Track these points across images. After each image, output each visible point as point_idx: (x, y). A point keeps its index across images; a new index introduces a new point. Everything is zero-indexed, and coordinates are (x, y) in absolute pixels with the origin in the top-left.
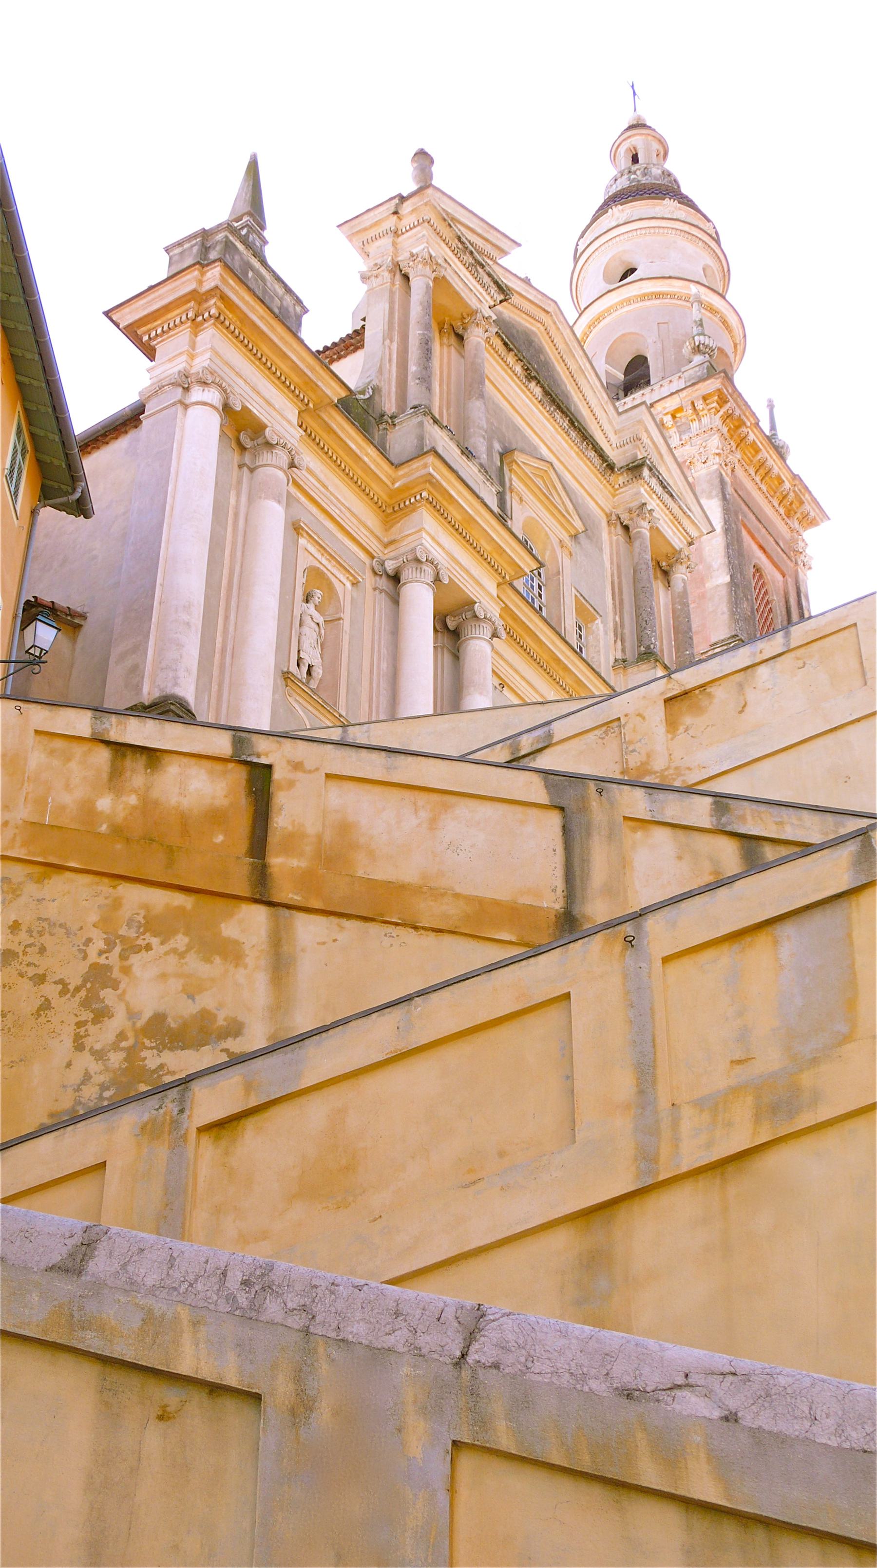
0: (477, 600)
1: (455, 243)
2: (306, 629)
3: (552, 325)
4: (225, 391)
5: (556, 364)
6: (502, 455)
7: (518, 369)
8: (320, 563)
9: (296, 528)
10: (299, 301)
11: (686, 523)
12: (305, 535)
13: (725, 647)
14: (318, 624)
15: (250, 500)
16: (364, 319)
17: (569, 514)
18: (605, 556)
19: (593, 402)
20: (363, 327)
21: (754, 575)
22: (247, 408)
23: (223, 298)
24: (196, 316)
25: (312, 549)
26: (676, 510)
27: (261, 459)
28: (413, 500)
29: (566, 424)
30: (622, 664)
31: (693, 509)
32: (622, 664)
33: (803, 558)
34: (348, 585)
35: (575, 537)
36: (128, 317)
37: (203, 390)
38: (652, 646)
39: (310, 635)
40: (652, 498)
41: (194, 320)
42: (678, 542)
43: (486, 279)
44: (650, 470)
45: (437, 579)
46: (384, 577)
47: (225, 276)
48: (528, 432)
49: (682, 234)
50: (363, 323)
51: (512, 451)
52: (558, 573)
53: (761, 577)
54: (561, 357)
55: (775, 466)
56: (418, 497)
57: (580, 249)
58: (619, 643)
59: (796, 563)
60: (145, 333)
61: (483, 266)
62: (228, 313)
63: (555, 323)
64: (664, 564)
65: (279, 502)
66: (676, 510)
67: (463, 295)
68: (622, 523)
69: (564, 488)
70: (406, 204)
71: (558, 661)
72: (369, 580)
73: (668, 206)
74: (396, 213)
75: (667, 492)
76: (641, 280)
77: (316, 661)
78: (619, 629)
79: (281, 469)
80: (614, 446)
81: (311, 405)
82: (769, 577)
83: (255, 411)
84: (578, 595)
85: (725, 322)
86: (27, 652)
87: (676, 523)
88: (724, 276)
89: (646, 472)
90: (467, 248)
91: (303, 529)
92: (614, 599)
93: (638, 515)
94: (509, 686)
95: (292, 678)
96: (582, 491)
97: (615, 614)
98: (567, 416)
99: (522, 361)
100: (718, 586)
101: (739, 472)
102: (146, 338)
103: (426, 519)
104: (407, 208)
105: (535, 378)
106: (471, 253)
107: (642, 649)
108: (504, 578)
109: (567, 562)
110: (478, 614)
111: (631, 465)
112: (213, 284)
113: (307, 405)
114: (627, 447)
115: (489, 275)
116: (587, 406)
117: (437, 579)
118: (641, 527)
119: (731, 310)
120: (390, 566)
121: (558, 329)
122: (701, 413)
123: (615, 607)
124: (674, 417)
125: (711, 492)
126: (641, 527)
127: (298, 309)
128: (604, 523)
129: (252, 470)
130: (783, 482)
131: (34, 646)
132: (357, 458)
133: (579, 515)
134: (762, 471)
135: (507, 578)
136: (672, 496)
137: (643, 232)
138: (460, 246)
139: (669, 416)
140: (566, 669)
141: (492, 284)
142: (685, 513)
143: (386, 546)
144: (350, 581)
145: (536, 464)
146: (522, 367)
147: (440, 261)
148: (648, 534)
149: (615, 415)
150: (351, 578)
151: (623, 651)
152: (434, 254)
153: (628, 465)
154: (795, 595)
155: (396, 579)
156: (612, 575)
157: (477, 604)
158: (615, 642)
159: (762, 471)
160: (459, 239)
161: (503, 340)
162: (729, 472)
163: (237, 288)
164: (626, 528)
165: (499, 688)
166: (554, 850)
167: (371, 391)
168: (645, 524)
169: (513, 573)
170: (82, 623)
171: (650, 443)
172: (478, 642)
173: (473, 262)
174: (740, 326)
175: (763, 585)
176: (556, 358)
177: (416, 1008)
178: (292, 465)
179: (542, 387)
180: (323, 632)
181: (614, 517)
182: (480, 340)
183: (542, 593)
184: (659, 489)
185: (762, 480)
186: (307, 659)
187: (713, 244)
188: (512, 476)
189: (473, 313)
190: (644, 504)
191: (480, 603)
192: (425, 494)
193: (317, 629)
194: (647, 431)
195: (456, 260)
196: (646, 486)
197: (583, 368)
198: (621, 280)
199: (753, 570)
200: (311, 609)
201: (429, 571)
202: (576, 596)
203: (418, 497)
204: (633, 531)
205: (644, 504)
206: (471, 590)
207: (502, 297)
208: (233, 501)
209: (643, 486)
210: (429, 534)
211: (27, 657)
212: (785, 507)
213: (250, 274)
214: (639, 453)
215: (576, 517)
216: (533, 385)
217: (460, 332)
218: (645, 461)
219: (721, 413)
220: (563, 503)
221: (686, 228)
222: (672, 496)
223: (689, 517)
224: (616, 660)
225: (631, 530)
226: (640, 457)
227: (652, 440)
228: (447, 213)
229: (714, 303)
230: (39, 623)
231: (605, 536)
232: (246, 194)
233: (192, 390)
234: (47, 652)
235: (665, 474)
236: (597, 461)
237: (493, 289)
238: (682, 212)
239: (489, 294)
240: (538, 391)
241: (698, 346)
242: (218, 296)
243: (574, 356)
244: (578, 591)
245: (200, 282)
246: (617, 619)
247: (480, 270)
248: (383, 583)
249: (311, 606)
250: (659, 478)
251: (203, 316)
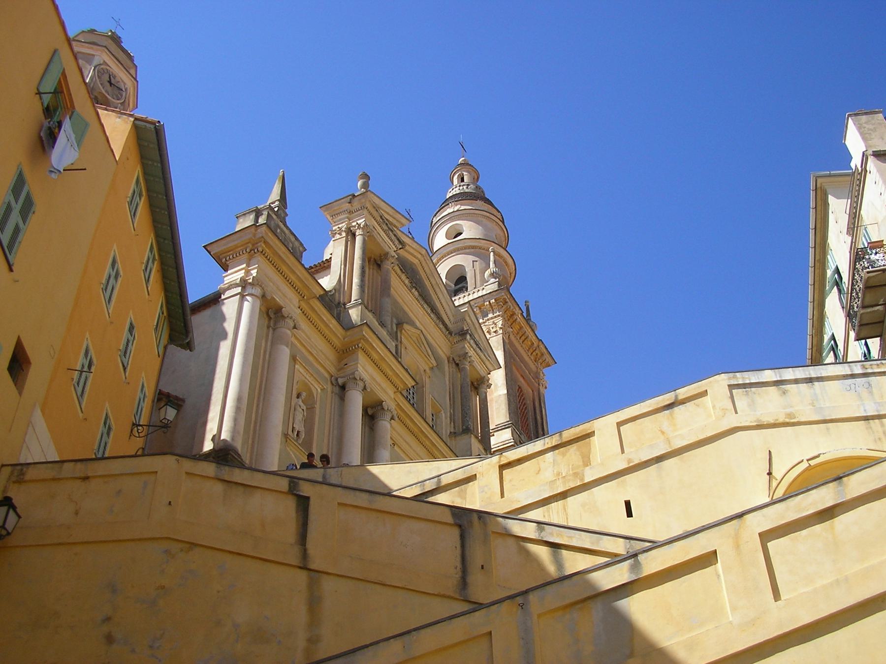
0: (384, 400)
1: (379, 219)
2: (297, 413)
3: (423, 260)
4: (263, 289)
5: (425, 281)
6: (397, 325)
7: (407, 282)
8: (306, 378)
9: (294, 359)
10: (301, 244)
11: (487, 363)
12: (299, 363)
13: (503, 427)
14: (303, 410)
15: (273, 344)
16: (331, 254)
17: (429, 356)
18: (446, 379)
19: (443, 301)
20: (331, 258)
21: (518, 390)
22: (274, 298)
23: (265, 242)
24: (251, 251)
25: (302, 370)
26: (482, 356)
27: (281, 324)
28: (353, 348)
29: (429, 311)
30: (454, 434)
31: (491, 356)
32: (454, 434)
33: (542, 382)
34: (319, 390)
35: (432, 369)
36: (215, 249)
37: (252, 288)
38: (469, 426)
39: (299, 416)
41: (249, 252)
42: (483, 373)
43: (393, 237)
44: (470, 336)
45: (365, 388)
46: (337, 387)
47: (267, 231)
48: (411, 314)
49: (486, 218)
50: (331, 256)
51: (402, 323)
52: (423, 387)
53: (521, 391)
54: (428, 277)
55: (530, 336)
56: (357, 346)
57: (434, 223)
58: (452, 424)
59: (539, 384)
60: (224, 257)
61: (392, 231)
62: (267, 250)
63: (425, 260)
64: (475, 383)
65: (287, 347)
66: (482, 356)
67: (382, 245)
68: (455, 362)
69: (428, 344)
70: (356, 198)
71: (422, 432)
72: (329, 387)
73: (480, 204)
74: (349, 203)
76: (465, 239)
77: (302, 429)
78: (453, 416)
79: (289, 329)
80: (452, 323)
81: (305, 297)
82: (525, 391)
83: (277, 299)
84: (433, 398)
85: (506, 262)
86: (161, 421)
87: (482, 363)
88: (506, 239)
89: (468, 337)
90: (384, 222)
91: (298, 360)
92: (450, 400)
93: (464, 359)
94: (397, 444)
95: (290, 438)
96: (436, 345)
97: (451, 408)
98: (430, 307)
99: (408, 278)
100: (500, 395)
101: (512, 337)
102: (224, 260)
103: (361, 356)
104: (356, 200)
106: (387, 224)
107: (464, 427)
108: (398, 389)
109: (427, 380)
110: (384, 407)
111: (461, 333)
112: (261, 235)
113: (303, 297)
114: (459, 324)
115: (395, 235)
116: (439, 302)
117: (365, 388)
118: (465, 365)
119: (509, 256)
120: (340, 381)
121: (427, 263)
122: (494, 307)
123: (450, 404)
124: (480, 309)
125: (498, 347)
126: (465, 365)
127: (301, 249)
128: (446, 362)
129: (274, 330)
130: (533, 343)
131: (165, 418)
132: (327, 325)
133: (434, 358)
134: (523, 338)
135: (399, 389)
136: (481, 349)
137: (466, 215)
138: (381, 220)
139: (478, 308)
140: (426, 437)
141: (396, 240)
143: (339, 370)
144: (320, 388)
145: (414, 330)
146: (409, 281)
147: (372, 228)
148: (468, 368)
149: (454, 307)
150: (321, 386)
151: (454, 427)
152: (368, 224)
153: (459, 333)
154: (538, 401)
155: (343, 388)
156: (450, 389)
157: (384, 402)
158: (450, 423)
159: (523, 338)
160: (381, 217)
161: (400, 267)
162: (507, 337)
163: (273, 238)
164: (457, 365)
165: (393, 445)
166: (456, 547)
167: (334, 291)
168: (467, 363)
169: (402, 387)
170: (183, 404)
171: (470, 322)
172: (384, 422)
173: (387, 228)
174: (513, 264)
175: (522, 396)
176: (425, 277)
177: (413, 637)
178: (295, 327)
179: (418, 292)
180: (305, 413)
181: (451, 359)
182: (389, 267)
183: (415, 397)
184: (475, 346)
185: (523, 342)
186: (297, 428)
187: (501, 223)
188: (402, 336)
189: (386, 255)
190: (467, 353)
191: (385, 401)
192: (360, 345)
193: (303, 412)
194: (469, 316)
195: (379, 228)
196: (468, 344)
198: (455, 238)
199: (518, 388)
200: (300, 402)
201: (361, 384)
202: (432, 399)
203: (357, 346)
204: (461, 366)
205: (467, 353)
206: (382, 396)
207: (401, 247)
208: (263, 345)
210: (361, 365)
211: (160, 424)
212: (534, 356)
213: (279, 231)
214: (465, 327)
215: (433, 358)
216: (414, 290)
217: (379, 263)
218: (468, 332)
219: (503, 308)
220: (427, 351)
221: (488, 214)
222: (481, 349)
224: (451, 433)
225: (460, 365)
226: (465, 329)
227: (472, 321)
228: (376, 204)
229: (501, 252)
230: (168, 407)
231: (447, 368)
232: (278, 191)
233: (246, 288)
234: (171, 422)
235: (477, 338)
236: (444, 330)
237: (397, 242)
238: (487, 207)
239: (394, 245)
240: (416, 293)
241: (493, 274)
242: (263, 241)
243: (434, 277)
244: (432, 396)
245: (254, 235)
246: (452, 411)
247: (391, 233)
248: (337, 389)
249: (300, 400)
251: (254, 250)
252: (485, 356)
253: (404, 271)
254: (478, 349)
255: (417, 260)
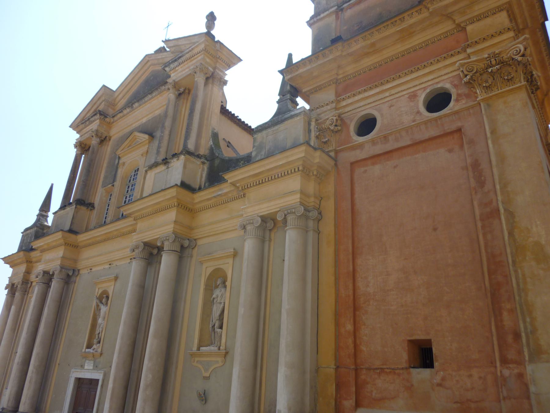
29: (150, 96)
40: (178, 70)
44: (166, 66)
61: (89, 119)
75: (179, 59)
105: (132, 105)
115: (92, 117)
138: (84, 124)
142: (190, 51)
173: (88, 121)
179: (135, 102)
196: (171, 72)
197: (161, 57)
207: (98, 115)
209: (171, 74)
222: (180, 57)
223: (192, 49)
237: (96, 117)
250: (170, 63)
252: (188, 52)
253: (120, 111)
254: (180, 60)
255: (151, 67)
